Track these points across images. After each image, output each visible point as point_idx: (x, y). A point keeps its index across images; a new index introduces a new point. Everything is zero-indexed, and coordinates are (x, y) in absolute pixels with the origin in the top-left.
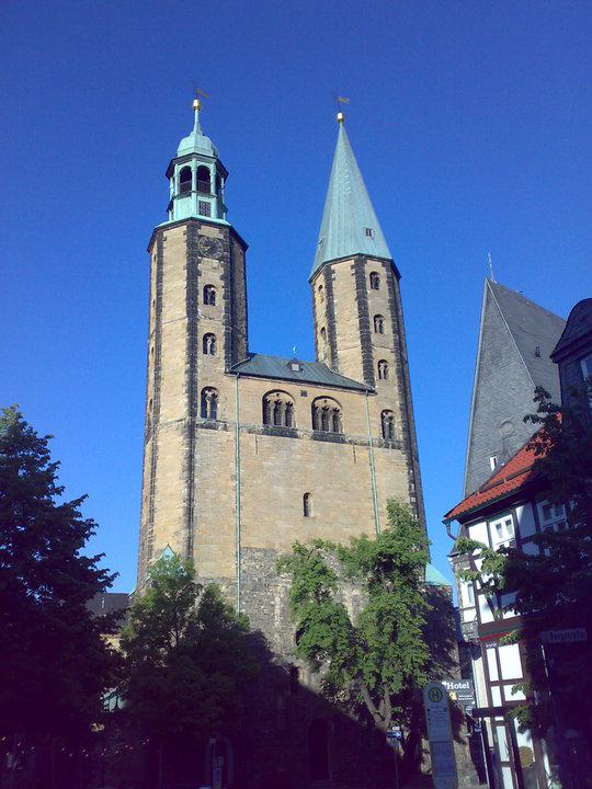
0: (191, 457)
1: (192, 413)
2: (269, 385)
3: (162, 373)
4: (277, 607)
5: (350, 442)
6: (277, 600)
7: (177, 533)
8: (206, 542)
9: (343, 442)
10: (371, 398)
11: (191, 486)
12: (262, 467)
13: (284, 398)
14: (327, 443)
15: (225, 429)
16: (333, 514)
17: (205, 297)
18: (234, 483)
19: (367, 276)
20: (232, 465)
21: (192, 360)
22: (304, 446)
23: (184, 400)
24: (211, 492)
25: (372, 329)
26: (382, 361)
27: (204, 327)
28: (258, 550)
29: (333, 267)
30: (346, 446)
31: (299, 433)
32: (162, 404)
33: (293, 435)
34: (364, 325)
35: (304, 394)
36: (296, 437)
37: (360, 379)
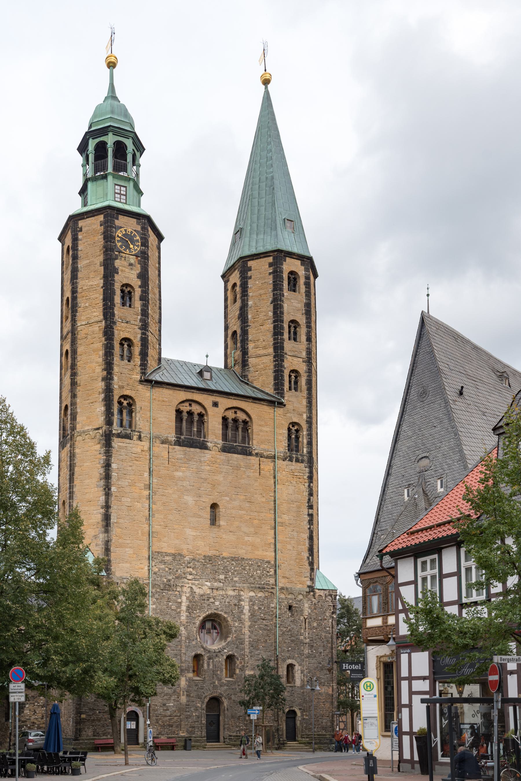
0: (107, 466)
1: (109, 422)
2: (183, 395)
3: (78, 379)
4: (183, 604)
5: (257, 454)
6: (184, 598)
7: (96, 537)
8: (121, 546)
9: (250, 454)
10: (279, 411)
11: (108, 494)
12: (172, 478)
13: (196, 409)
14: (235, 456)
15: (140, 438)
16: (237, 523)
17: (123, 297)
18: (146, 493)
19: (285, 276)
20: (146, 474)
21: (109, 367)
22: (212, 457)
23: (101, 408)
24: (126, 500)
25: (286, 336)
26: (293, 371)
27: (121, 331)
28: (167, 554)
29: (250, 263)
30: (254, 460)
31: (209, 444)
32: (79, 410)
33: (203, 446)
34: (277, 332)
35: (215, 404)
36: (206, 448)
37: (270, 389)
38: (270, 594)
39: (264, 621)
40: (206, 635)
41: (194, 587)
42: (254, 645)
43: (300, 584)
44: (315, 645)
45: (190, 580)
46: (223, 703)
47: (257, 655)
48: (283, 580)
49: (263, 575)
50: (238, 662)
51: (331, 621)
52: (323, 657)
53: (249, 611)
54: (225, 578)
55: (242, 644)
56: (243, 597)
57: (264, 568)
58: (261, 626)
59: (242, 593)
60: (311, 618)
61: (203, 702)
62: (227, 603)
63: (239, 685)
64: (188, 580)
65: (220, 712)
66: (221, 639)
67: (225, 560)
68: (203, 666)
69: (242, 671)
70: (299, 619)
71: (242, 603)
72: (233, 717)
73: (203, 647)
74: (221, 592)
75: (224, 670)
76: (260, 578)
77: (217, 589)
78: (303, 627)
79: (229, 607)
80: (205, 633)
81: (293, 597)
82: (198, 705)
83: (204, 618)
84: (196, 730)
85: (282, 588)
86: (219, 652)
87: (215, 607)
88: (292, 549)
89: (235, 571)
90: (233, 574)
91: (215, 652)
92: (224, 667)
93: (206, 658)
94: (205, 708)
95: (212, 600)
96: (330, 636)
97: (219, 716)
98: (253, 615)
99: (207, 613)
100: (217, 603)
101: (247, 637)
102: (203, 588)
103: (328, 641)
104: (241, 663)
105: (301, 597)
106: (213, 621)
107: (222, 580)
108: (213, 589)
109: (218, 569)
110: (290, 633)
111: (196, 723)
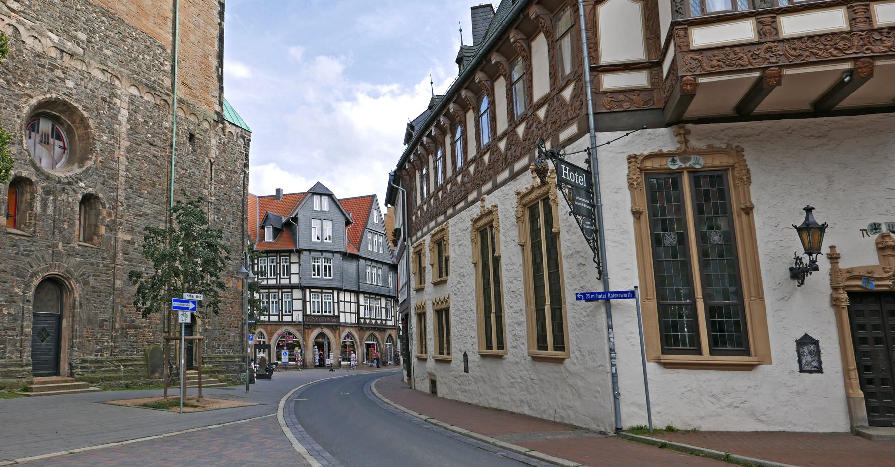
38: (162, 103)
39: (152, 148)
40: (39, 146)
41: (21, 29)
42: (134, 185)
43: (206, 104)
44: (222, 209)
45: (13, 11)
46: (72, 291)
47: (139, 205)
48: (183, 88)
49: (154, 66)
50: (105, 212)
51: (242, 176)
52: (231, 230)
53: (129, 121)
54: (89, 41)
55: (113, 179)
56: (119, 92)
57: (155, 54)
58: (146, 154)
59: (117, 82)
60: (218, 164)
61: (27, 286)
62: (88, 91)
63: (104, 258)
64: (9, 8)
65: (61, 311)
66: (70, 162)
67: (91, 9)
68: (31, 206)
69: (111, 230)
70: (203, 161)
71: (117, 101)
72: (90, 321)
73: (34, 165)
74: (79, 66)
75: (77, 222)
76: (148, 69)
77: (71, 55)
78: (208, 175)
79: (92, 100)
80: (38, 140)
81: (197, 122)
82: (17, 290)
83: (41, 105)
84: (9, 348)
85: (181, 101)
86: (69, 183)
87: (64, 90)
88: (196, 43)
89: (108, 37)
90: (102, 39)
91: (59, 182)
92: (76, 216)
93: (39, 190)
94: (32, 299)
95: (58, 72)
96: (240, 199)
97: (59, 318)
98: (133, 130)
99: (48, 96)
100: (70, 84)
101: (122, 167)
102: (43, 40)
103: (238, 206)
104: (110, 215)
105: (206, 125)
106: (55, 119)
107: (82, 41)
108: (62, 51)
109: (77, 18)
110: (189, 180)
111: (10, 332)
